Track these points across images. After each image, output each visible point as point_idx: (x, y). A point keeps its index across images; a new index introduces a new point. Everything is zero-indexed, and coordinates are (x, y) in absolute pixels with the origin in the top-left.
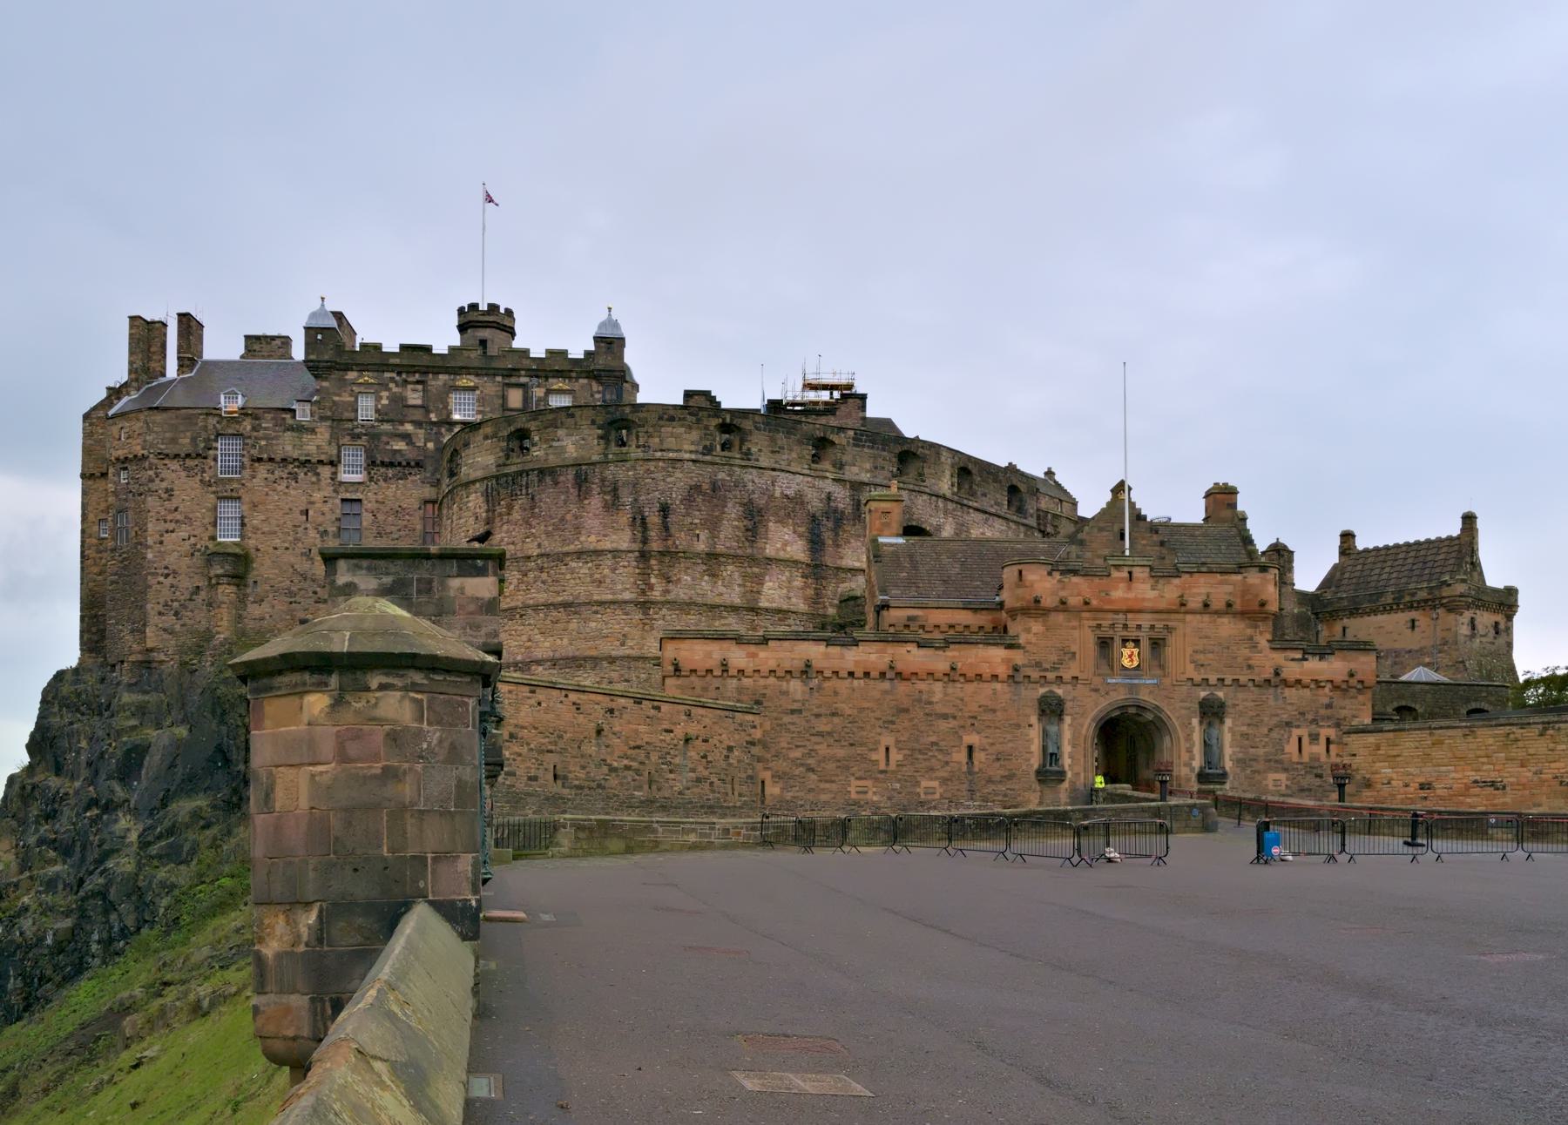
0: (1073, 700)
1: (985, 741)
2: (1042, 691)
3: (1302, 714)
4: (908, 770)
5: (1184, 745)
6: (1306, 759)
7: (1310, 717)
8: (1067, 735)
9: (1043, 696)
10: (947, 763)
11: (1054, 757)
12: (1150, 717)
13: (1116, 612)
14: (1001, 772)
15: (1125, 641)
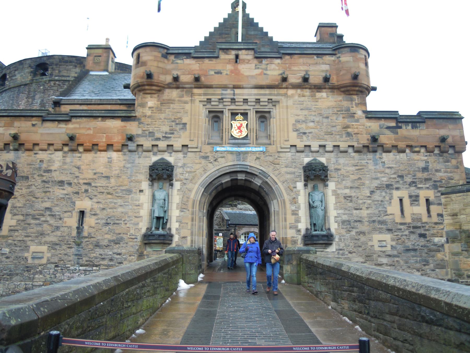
0: (184, 166)
1: (96, 206)
2: (155, 159)
3: (401, 177)
4: (19, 235)
5: (290, 208)
6: (408, 219)
7: (408, 179)
8: (176, 199)
9: (155, 164)
10: (58, 228)
11: (161, 221)
12: (258, 182)
13: (225, 87)
14: (108, 237)
15: (234, 115)
